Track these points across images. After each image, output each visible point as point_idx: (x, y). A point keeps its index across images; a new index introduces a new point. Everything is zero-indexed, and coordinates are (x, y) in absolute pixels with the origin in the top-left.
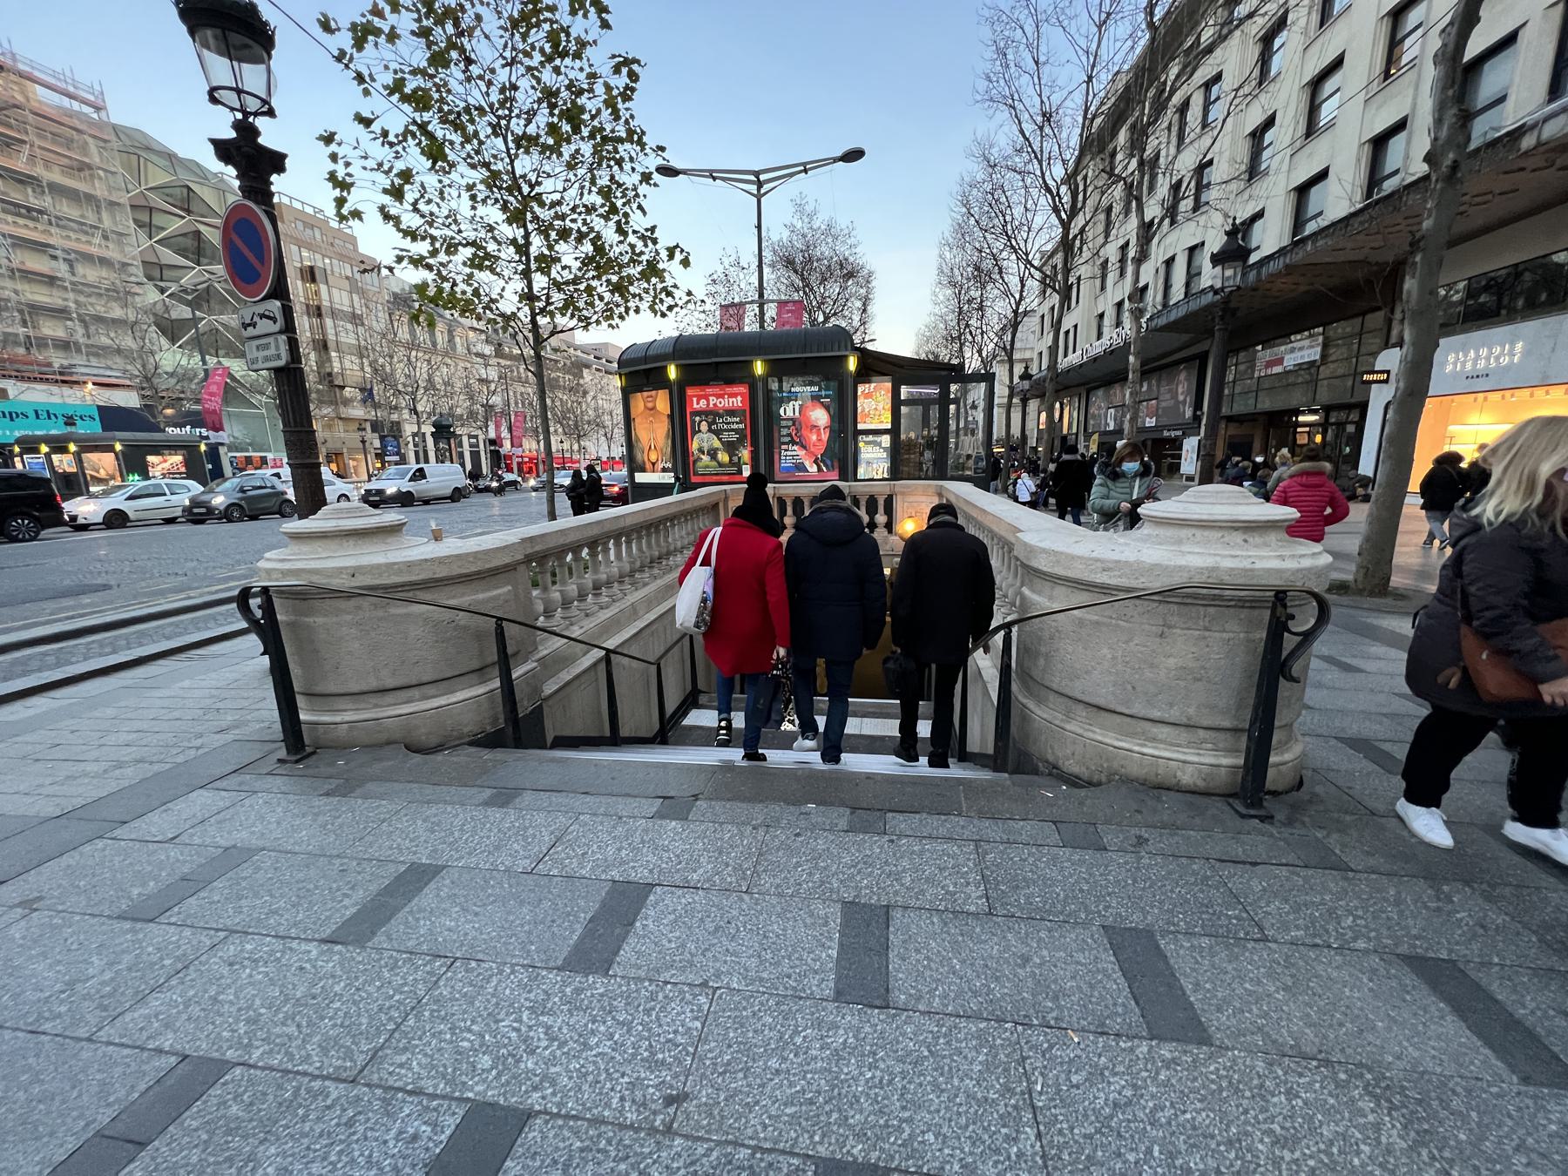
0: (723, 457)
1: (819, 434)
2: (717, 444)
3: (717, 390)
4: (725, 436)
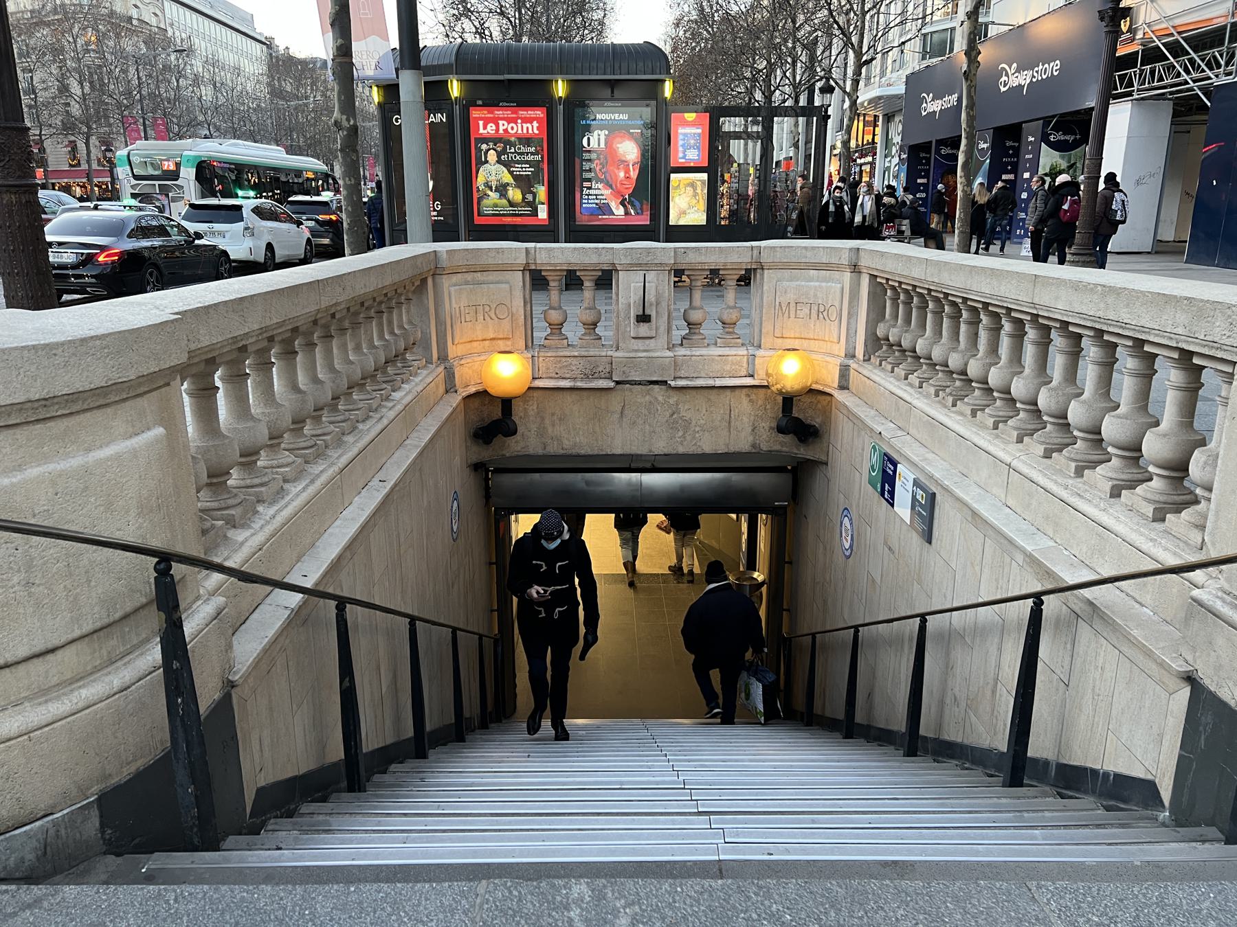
0: (515, 194)
1: (627, 171)
2: (508, 178)
3: (508, 113)
4: (517, 169)
